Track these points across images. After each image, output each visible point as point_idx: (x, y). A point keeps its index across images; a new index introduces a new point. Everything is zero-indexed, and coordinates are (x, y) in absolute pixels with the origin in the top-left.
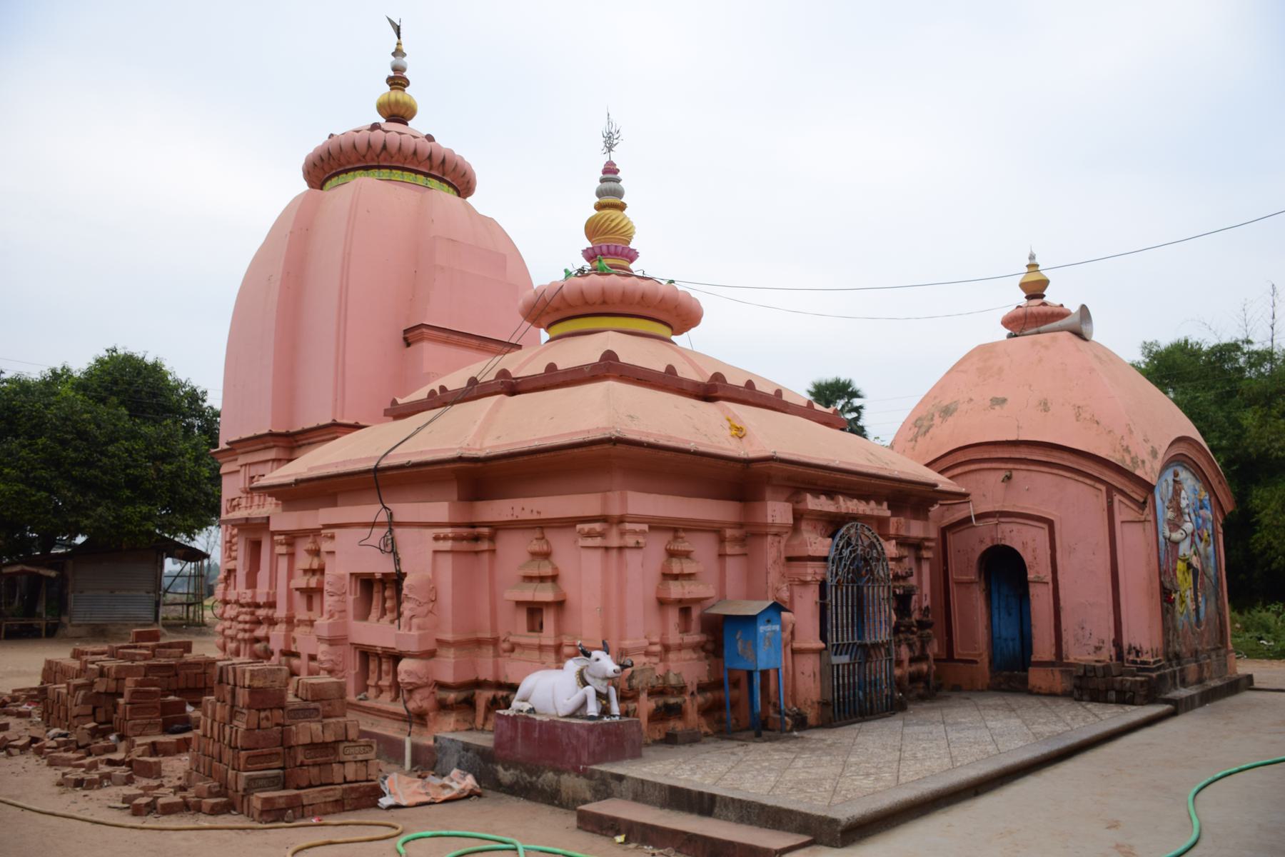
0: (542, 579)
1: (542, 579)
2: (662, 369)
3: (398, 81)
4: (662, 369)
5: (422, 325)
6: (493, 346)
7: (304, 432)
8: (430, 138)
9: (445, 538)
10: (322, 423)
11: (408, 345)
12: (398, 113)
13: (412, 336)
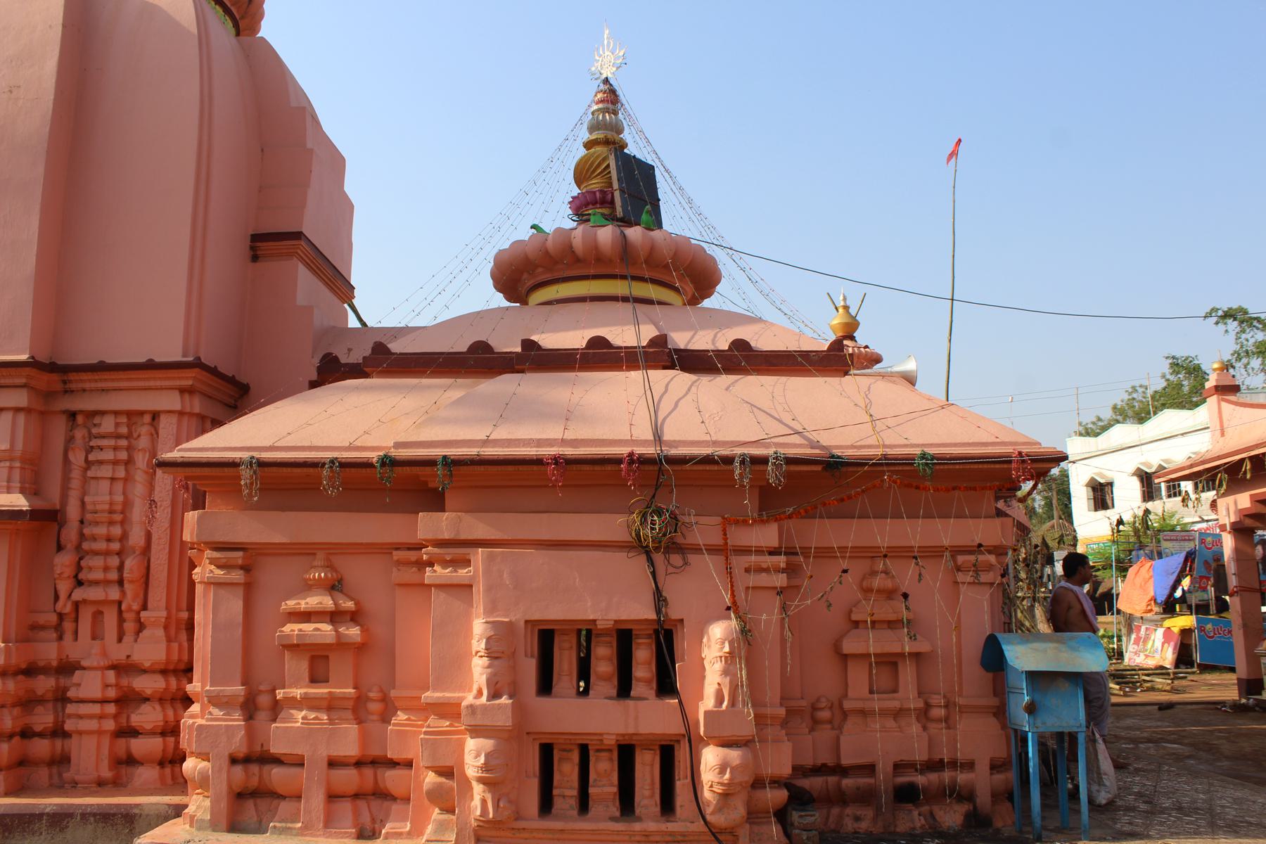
0: (893, 624)
1: (893, 624)
5: (298, 235)
10: (157, 360)
11: (255, 258)
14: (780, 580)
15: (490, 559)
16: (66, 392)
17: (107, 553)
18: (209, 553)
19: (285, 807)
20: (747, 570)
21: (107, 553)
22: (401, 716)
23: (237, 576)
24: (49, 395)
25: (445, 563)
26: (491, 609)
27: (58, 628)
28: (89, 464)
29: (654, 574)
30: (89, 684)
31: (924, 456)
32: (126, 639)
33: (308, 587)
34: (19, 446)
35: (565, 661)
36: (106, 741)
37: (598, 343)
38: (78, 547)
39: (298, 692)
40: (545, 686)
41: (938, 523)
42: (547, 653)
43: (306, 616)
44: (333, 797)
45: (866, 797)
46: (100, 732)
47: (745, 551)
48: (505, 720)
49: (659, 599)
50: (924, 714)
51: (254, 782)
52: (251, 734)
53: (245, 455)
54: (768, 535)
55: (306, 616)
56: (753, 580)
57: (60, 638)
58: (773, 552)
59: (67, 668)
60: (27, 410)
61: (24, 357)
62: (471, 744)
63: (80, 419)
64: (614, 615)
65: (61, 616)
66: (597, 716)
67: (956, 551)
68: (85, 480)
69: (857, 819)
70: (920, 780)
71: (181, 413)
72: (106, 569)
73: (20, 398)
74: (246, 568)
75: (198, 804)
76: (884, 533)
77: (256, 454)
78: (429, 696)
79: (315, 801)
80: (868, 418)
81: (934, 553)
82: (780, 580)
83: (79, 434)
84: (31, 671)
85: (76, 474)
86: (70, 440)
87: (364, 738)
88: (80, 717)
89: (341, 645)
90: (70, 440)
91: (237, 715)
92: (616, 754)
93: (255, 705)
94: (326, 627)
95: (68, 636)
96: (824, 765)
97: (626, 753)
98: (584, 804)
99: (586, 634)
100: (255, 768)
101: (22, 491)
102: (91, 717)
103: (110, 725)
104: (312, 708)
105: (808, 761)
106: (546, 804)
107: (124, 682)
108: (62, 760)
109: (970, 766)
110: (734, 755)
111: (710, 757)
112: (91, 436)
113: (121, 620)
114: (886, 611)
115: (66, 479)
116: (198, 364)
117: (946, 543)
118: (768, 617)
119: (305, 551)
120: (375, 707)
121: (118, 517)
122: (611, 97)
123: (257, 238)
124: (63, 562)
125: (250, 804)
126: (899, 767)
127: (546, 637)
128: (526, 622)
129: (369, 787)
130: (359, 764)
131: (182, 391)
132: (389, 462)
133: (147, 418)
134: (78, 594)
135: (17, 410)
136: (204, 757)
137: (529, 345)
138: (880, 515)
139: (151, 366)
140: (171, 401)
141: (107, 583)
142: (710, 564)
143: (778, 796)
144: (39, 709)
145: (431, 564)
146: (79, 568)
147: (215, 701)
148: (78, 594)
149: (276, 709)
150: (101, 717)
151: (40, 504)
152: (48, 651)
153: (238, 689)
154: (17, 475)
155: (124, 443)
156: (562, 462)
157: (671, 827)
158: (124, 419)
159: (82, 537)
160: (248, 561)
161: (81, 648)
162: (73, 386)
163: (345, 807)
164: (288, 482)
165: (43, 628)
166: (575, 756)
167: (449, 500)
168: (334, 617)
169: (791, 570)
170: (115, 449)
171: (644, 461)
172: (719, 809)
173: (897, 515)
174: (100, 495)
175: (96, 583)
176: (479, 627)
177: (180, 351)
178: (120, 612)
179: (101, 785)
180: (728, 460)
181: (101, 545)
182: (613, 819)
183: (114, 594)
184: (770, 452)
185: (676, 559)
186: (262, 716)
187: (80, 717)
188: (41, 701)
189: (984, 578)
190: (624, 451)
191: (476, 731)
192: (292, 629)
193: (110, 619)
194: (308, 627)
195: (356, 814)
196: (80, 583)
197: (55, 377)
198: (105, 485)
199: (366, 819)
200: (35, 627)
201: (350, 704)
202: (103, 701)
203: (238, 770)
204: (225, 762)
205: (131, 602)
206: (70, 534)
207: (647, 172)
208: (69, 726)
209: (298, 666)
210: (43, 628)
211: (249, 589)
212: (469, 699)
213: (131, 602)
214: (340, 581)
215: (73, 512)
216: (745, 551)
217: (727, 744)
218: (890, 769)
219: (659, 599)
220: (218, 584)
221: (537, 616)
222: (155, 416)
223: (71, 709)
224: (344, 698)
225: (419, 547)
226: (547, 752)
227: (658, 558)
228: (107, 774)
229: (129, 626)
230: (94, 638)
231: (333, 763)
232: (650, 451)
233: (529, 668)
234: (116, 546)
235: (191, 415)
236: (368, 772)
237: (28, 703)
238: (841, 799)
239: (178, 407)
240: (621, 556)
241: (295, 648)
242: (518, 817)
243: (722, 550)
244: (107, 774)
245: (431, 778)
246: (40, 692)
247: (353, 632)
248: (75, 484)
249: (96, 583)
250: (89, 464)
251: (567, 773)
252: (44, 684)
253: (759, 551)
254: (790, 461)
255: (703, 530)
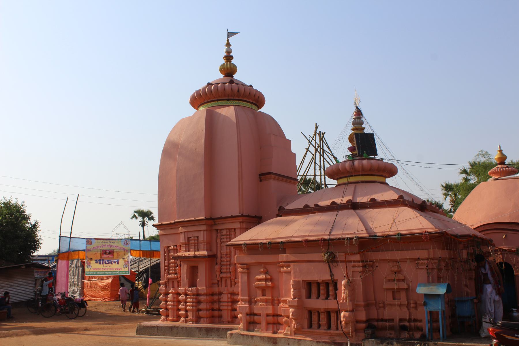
0: (398, 280)
1: (398, 280)
2: (411, 200)
3: (229, 58)
4: (411, 200)
5: (270, 173)
6: (290, 180)
7: (221, 218)
8: (251, 86)
9: (359, 266)
11: (261, 181)
12: (229, 71)
13: (263, 176)
14: (360, 269)
15: (294, 265)
16: (215, 224)
17: (227, 265)
18: (240, 266)
19: (258, 325)
20: (353, 267)
21: (227, 265)
22: (282, 304)
23: (245, 271)
24: (211, 226)
25: (286, 267)
26: (295, 278)
27: (218, 284)
28: (221, 243)
29: (330, 268)
30: (225, 298)
31: (398, 234)
32: (233, 286)
33: (261, 273)
34: (205, 239)
35: (314, 290)
36: (229, 311)
37: (333, 203)
38: (221, 264)
39: (259, 298)
40: (309, 296)
41: (405, 252)
42: (310, 288)
43: (260, 280)
44: (268, 323)
45: (392, 328)
46: (228, 310)
47: (351, 262)
48: (296, 304)
49: (332, 275)
50: (408, 305)
51: (252, 320)
52: (251, 308)
53: (243, 242)
54: (357, 257)
55: (260, 280)
56: (352, 269)
57: (218, 286)
58: (359, 262)
59: (220, 294)
60: (206, 230)
61: (203, 218)
62: (291, 310)
63: (219, 231)
64: (322, 279)
65: (218, 281)
66: (319, 304)
67: (412, 260)
68: (221, 246)
69: (391, 334)
70: (407, 324)
71: (240, 228)
72: (227, 269)
73: (204, 228)
74: (248, 269)
75: (241, 325)
76: (397, 255)
77: (246, 242)
78: (284, 298)
79: (264, 324)
80: (392, 222)
81: (405, 260)
82: (360, 269)
83: (219, 235)
84: (213, 294)
85: (219, 245)
86: (217, 236)
87: (274, 309)
88: (223, 306)
89: (267, 287)
90: (217, 236)
91: (247, 304)
92: (326, 314)
93: (251, 302)
94: (264, 282)
95: (220, 286)
96: (382, 319)
97: (328, 313)
98: (319, 326)
99: (318, 284)
100: (252, 316)
101: (207, 251)
102: (225, 306)
103: (230, 308)
104: (263, 302)
105: (375, 317)
106: (310, 326)
107: (233, 297)
108: (220, 317)
109: (420, 321)
110: (347, 314)
111: (342, 314)
112: (221, 235)
113: (231, 282)
114: (395, 277)
115: (217, 247)
116: (243, 216)
117: (408, 258)
118: (358, 279)
119: (259, 264)
120: (276, 302)
121: (228, 256)
122: (359, 113)
123: (260, 175)
124: (217, 267)
125: (252, 325)
126: (401, 320)
127: (309, 284)
128: (303, 281)
129: (275, 322)
130: (274, 316)
131: (240, 222)
132: (270, 243)
133: (233, 230)
134: (221, 275)
135: (204, 230)
136: (241, 313)
137: (316, 205)
138: (387, 251)
139: (232, 217)
140: (237, 225)
141: (227, 272)
142: (341, 266)
143: (363, 325)
144: (215, 304)
145: (283, 267)
146: (221, 269)
147: (243, 300)
148: (221, 275)
149: (256, 302)
150: (228, 306)
151: (211, 253)
152: (216, 290)
153: (247, 297)
154: (205, 246)
155: (228, 237)
156: (307, 241)
157: (337, 332)
158: (228, 231)
159: (221, 261)
160: (248, 267)
161: (223, 289)
162: (216, 223)
163: (271, 326)
164: (252, 248)
165: (215, 284)
166: (317, 314)
167: (287, 251)
168: (266, 280)
169: (364, 266)
170: (227, 238)
171: (324, 240)
172: (345, 328)
173: (392, 250)
174: (225, 250)
175: (224, 272)
176: (291, 282)
177: (238, 212)
178: (231, 280)
179: (229, 323)
180: (344, 239)
181: (225, 263)
182: (325, 330)
183: (229, 275)
184: (354, 236)
185: (335, 264)
186: (253, 304)
187: (223, 306)
188: (215, 302)
189: (420, 267)
190: (320, 238)
191: (291, 307)
192: (257, 283)
193: (229, 282)
194: (260, 283)
195: (273, 328)
196: (222, 273)
197: (212, 221)
198: (225, 248)
199: (275, 329)
200: (213, 284)
201: (271, 301)
202: (228, 302)
203: (248, 317)
204: (245, 315)
205: (233, 277)
206: (219, 260)
207: (371, 137)
208: (221, 308)
209: (259, 292)
210: (215, 284)
211: (249, 274)
212: (290, 300)
213: (233, 277)
214: (268, 271)
215: (219, 255)
216: (351, 262)
217: (346, 311)
218: (398, 320)
219: (332, 275)
220: (242, 273)
221: (304, 279)
222: (235, 229)
223: (221, 304)
224: (269, 300)
225: (280, 262)
226: (310, 312)
227: (331, 264)
228: (230, 320)
229: (233, 283)
230: (226, 286)
231: (268, 315)
232: (326, 237)
233: (304, 292)
234: (228, 263)
235: (243, 228)
236: (276, 318)
237: (213, 302)
238: (384, 329)
239: (239, 227)
240: (321, 264)
241: (258, 287)
242: (303, 328)
243: (345, 262)
244: (230, 320)
245: (285, 319)
246: (215, 300)
247: (269, 283)
248: (219, 248)
249: (224, 272)
250: (221, 243)
251: (315, 317)
252: (216, 298)
253: (354, 262)
254: (359, 238)
255: (341, 256)
